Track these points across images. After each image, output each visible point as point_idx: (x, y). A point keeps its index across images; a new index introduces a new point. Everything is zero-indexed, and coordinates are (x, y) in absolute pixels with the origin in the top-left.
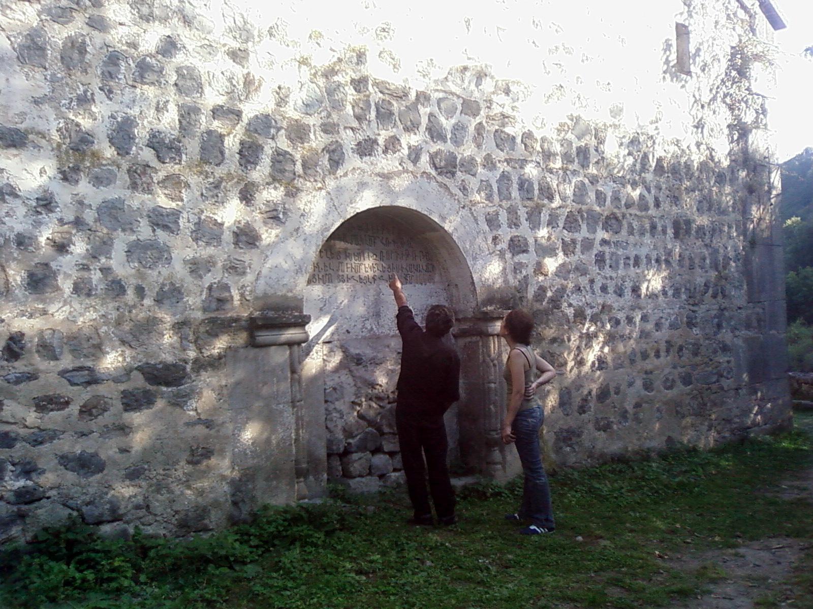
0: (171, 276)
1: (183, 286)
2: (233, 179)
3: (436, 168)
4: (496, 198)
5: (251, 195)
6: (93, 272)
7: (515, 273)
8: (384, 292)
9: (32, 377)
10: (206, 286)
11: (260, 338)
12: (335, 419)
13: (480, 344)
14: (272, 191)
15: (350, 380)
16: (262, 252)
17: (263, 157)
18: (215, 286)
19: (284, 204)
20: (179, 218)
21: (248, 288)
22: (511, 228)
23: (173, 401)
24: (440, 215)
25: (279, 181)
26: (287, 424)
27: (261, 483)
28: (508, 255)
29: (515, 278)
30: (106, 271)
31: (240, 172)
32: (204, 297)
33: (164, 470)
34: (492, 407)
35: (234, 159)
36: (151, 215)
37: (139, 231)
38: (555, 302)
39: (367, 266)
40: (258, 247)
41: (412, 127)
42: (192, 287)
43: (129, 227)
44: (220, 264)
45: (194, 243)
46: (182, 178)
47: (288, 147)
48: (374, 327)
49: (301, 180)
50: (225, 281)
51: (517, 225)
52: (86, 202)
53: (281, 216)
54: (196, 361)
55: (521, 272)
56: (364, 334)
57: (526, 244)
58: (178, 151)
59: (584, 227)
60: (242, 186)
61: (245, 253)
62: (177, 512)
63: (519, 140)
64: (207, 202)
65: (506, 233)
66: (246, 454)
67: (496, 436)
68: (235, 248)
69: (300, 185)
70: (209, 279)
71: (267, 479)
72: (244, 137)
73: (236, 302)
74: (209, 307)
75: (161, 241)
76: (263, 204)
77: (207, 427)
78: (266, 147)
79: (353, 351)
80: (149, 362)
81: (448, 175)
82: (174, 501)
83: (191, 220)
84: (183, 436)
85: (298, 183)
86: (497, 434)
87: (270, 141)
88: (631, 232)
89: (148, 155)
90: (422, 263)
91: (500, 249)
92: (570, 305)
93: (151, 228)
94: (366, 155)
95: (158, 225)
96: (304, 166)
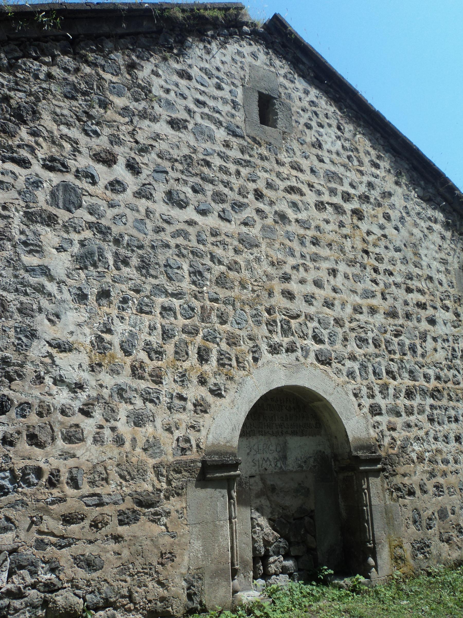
4: (358, 379)
6: (105, 429)
7: (375, 428)
9: (62, 500)
12: (258, 531)
13: (355, 478)
15: (268, 503)
27: (207, 580)
28: (369, 416)
29: (375, 431)
30: (113, 429)
33: (143, 569)
38: (403, 448)
41: (304, 336)
43: (129, 401)
51: (373, 397)
52: (104, 385)
53: (223, 393)
54: (167, 490)
56: (276, 471)
57: (381, 410)
59: (418, 396)
63: (370, 341)
65: (367, 402)
66: (198, 558)
70: (177, 434)
77: (172, 537)
79: (269, 483)
82: (148, 592)
88: (450, 399)
89: (143, 356)
92: (414, 450)
95: (147, 399)
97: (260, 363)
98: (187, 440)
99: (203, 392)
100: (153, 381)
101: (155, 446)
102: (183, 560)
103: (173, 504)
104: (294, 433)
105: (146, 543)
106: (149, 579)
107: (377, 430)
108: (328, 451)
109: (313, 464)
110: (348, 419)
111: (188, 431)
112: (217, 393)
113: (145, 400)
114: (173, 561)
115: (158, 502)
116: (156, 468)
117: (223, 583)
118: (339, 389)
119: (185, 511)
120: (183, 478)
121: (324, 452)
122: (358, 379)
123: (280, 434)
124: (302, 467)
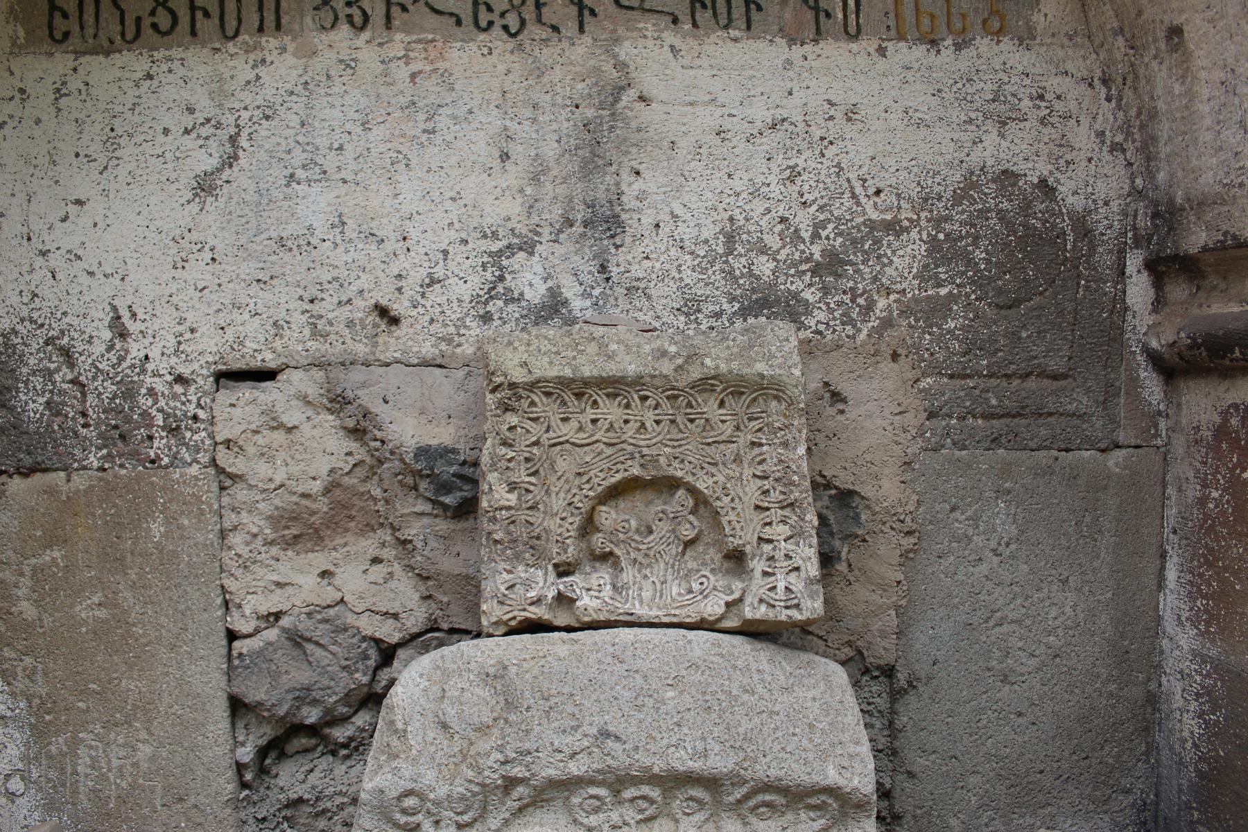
8: (649, 82)
48: (570, 291)
79: (408, 431)
108: (1094, 185)
109: (911, 286)
121: (1046, 188)
124: (793, 310)
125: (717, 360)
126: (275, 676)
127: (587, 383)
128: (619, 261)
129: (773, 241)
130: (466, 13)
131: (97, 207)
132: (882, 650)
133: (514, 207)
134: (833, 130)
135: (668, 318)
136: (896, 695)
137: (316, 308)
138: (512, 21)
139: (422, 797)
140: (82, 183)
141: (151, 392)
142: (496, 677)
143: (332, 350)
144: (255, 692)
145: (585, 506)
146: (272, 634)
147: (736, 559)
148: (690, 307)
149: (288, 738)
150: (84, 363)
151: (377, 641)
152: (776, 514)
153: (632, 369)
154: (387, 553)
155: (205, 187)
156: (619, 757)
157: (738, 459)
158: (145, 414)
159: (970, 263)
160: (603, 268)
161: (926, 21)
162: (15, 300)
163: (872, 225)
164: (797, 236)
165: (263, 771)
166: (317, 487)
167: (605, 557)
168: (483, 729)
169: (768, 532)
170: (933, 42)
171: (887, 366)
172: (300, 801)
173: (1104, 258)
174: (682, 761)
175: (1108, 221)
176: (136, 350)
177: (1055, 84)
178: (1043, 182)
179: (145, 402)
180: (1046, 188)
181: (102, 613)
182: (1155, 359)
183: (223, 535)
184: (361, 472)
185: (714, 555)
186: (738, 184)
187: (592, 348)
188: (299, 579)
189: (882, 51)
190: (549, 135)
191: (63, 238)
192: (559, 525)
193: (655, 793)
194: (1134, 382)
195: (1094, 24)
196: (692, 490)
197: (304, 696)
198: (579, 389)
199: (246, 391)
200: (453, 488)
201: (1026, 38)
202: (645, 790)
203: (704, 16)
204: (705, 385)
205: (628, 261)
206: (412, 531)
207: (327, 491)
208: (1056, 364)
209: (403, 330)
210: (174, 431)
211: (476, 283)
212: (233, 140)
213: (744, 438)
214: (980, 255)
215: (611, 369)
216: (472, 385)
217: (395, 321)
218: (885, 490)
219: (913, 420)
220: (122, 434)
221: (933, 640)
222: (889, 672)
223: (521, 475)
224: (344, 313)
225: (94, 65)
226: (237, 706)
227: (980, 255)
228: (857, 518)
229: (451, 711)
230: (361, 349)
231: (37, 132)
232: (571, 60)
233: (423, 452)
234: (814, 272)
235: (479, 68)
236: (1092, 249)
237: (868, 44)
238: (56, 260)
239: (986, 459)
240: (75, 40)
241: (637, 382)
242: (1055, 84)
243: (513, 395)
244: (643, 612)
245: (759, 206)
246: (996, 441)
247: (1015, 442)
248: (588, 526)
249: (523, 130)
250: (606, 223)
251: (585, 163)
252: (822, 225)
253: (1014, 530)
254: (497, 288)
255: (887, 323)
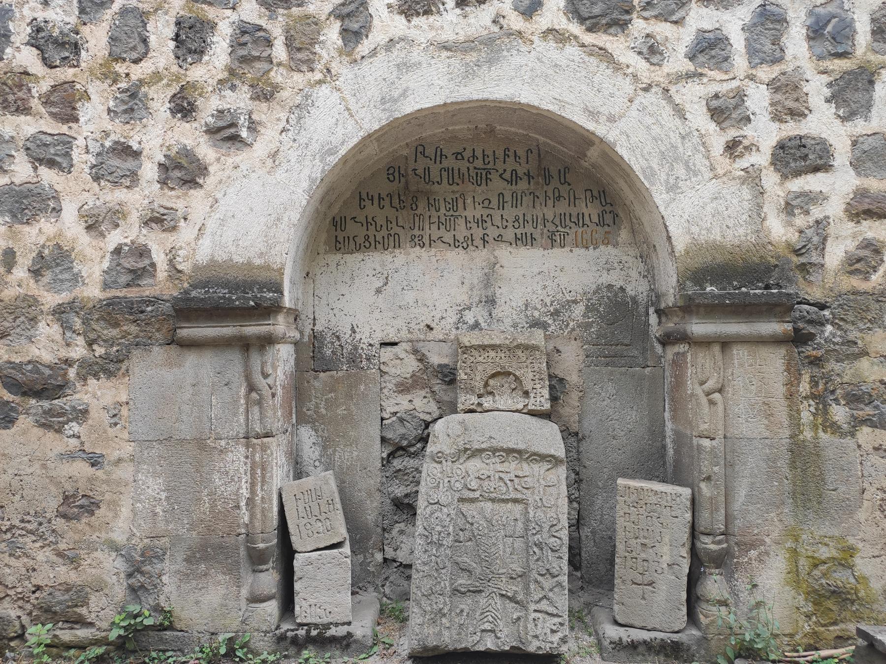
0: (60, 234)
1: (73, 249)
2: (162, 79)
3: (582, 20)
5: (189, 103)
8: (503, 261)
10: (111, 248)
11: (185, 330)
14: (228, 93)
16: (208, 195)
17: (214, 39)
18: (127, 248)
19: (250, 114)
20: (71, 148)
21: (180, 252)
22: (781, 121)
23: (43, 421)
24: (586, 109)
25: (241, 77)
26: (231, 473)
31: (175, 69)
32: (106, 265)
33: (22, 521)
34: (703, 485)
35: (165, 49)
36: (29, 144)
37: (12, 171)
39: (470, 219)
40: (201, 186)
42: (89, 251)
44: (134, 218)
45: (95, 184)
46: (78, 86)
47: (260, 17)
48: (481, 321)
49: (281, 69)
50: (142, 240)
53: (244, 134)
55: (807, 213)
58: (76, 48)
60: (175, 88)
61: (178, 197)
62: (38, 588)
64: (117, 121)
65: (765, 133)
66: (155, 514)
67: (713, 547)
68: (162, 188)
69: (279, 79)
70: (115, 238)
71: (188, 560)
72: (182, 13)
73: (162, 272)
74: (115, 282)
75: (45, 183)
76: (213, 115)
77: (93, 465)
78: (220, 24)
79: (435, 360)
80: (13, 360)
81: (612, 30)
82: (34, 570)
83: (92, 150)
84: (54, 474)
85: (277, 76)
86: (713, 543)
87: (228, 12)
90: (591, 211)
91: (746, 165)
93: (30, 165)
94: (418, 14)
95: (41, 161)
96: (289, 43)
97: (365, 47)
98: (142, 252)
99: (190, 136)
100: (53, 115)
101: (58, 265)
102: (116, 516)
103: (97, 394)
104: (524, 240)
105: (29, 471)
106: (38, 545)
107: (800, 221)
108: (637, 288)
109: (580, 319)
110: (673, 188)
111: (144, 231)
112: (227, 133)
113: (38, 161)
114: (92, 513)
115: (61, 387)
116: (59, 312)
117: (220, 577)
118: (652, 99)
119: (124, 411)
120: (123, 337)
121: (622, 289)
122: (740, 62)
123: (478, 242)
124: (544, 326)
125: (521, 340)
126: (395, 431)
127: (486, 346)
128: (495, 313)
129: (539, 307)
130: (452, 245)
131: (348, 297)
132: (575, 427)
133: (465, 297)
134: (557, 274)
135: (508, 328)
136: (579, 441)
137: (410, 325)
138: (465, 245)
139: (443, 453)
140: (344, 289)
141: (362, 348)
142: (462, 423)
143: (413, 337)
144: (389, 435)
145: (485, 379)
146: (394, 419)
147: (526, 394)
148: (515, 326)
149: (397, 450)
150: (343, 340)
151: (424, 421)
152: (537, 382)
153: (498, 343)
154: (428, 395)
155: (378, 291)
156: (494, 444)
157: (527, 367)
158: (360, 355)
159: (598, 312)
160: (490, 314)
161: (585, 241)
162: (324, 322)
163: (568, 301)
164: (546, 305)
165: (388, 462)
166: (408, 376)
167: (491, 393)
168: (458, 436)
169: (535, 386)
170: (587, 248)
171: (573, 342)
172: (400, 470)
173: (642, 309)
174: (511, 445)
175: (642, 298)
176: (358, 337)
177: (625, 258)
178: (621, 287)
179: (360, 351)
180: (622, 289)
181: (345, 412)
182: (658, 339)
183: (381, 389)
184: (421, 372)
185: (520, 393)
186: (529, 290)
187: (487, 337)
188: (402, 402)
189: (571, 251)
190: (475, 277)
191: (338, 305)
192: (479, 385)
193: (504, 454)
194: (653, 347)
195: (637, 240)
196: (515, 375)
197: (403, 437)
198: (484, 348)
199: (389, 349)
200: (448, 376)
201: (616, 245)
202: (502, 453)
203: (519, 242)
204: (518, 347)
205: (497, 312)
206: (436, 388)
207: (411, 377)
208: (626, 341)
209: (434, 331)
210: (368, 360)
211: (455, 318)
212: (387, 278)
213: (529, 361)
214: (601, 309)
215: (493, 342)
216: (453, 347)
217: (432, 329)
218: (573, 378)
219: (581, 358)
220: (353, 360)
221: (590, 425)
222: (577, 434)
223: (468, 371)
224: (418, 327)
225: (348, 257)
226: (383, 440)
227: (601, 309)
228: (565, 387)
229: (450, 432)
230: (422, 337)
231: (331, 275)
232: (481, 256)
233: (440, 366)
234: (551, 315)
235: (455, 258)
236: (638, 307)
237: (567, 249)
238: (336, 311)
239: (604, 370)
240: (342, 250)
241: (500, 346)
242: (625, 258)
243: (466, 349)
244: (501, 407)
245: (535, 296)
246: (607, 365)
247: (614, 365)
248: (486, 385)
249: (468, 276)
250: (491, 302)
251: (485, 285)
252: (553, 302)
253: (615, 392)
254: (461, 320)
255: (573, 330)
